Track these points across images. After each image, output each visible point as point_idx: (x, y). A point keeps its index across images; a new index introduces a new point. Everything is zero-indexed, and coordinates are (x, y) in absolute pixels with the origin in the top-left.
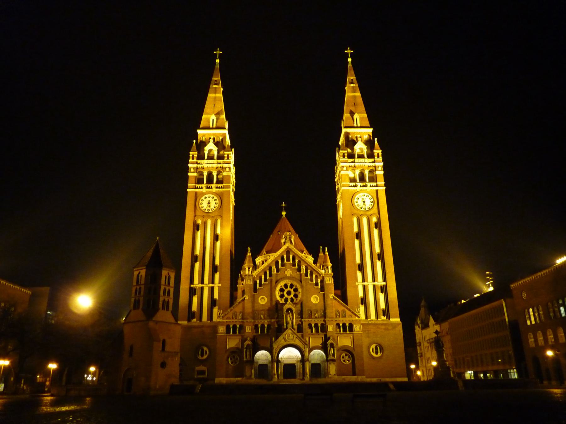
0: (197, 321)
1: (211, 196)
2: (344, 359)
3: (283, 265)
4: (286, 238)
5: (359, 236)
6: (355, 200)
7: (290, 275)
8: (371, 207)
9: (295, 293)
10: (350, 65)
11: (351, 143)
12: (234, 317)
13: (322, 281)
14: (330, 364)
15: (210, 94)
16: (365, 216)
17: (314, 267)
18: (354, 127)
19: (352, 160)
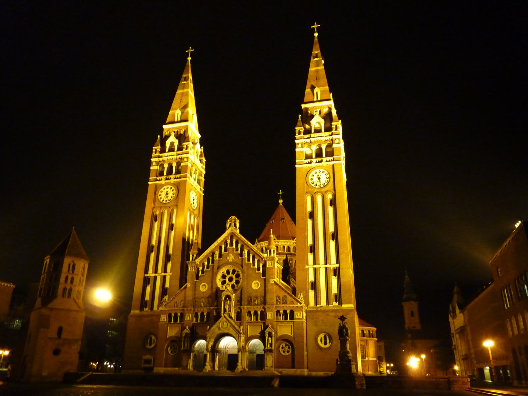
0: (148, 309)
1: (170, 186)
2: (283, 350)
3: (226, 250)
4: (231, 222)
5: (312, 215)
6: (310, 177)
7: (232, 260)
8: (326, 184)
9: (236, 279)
10: (316, 40)
11: (308, 117)
12: (176, 306)
13: (264, 266)
14: (267, 355)
15: (179, 90)
16: (320, 193)
17: (256, 251)
18: (313, 102)
19: (308, 136)
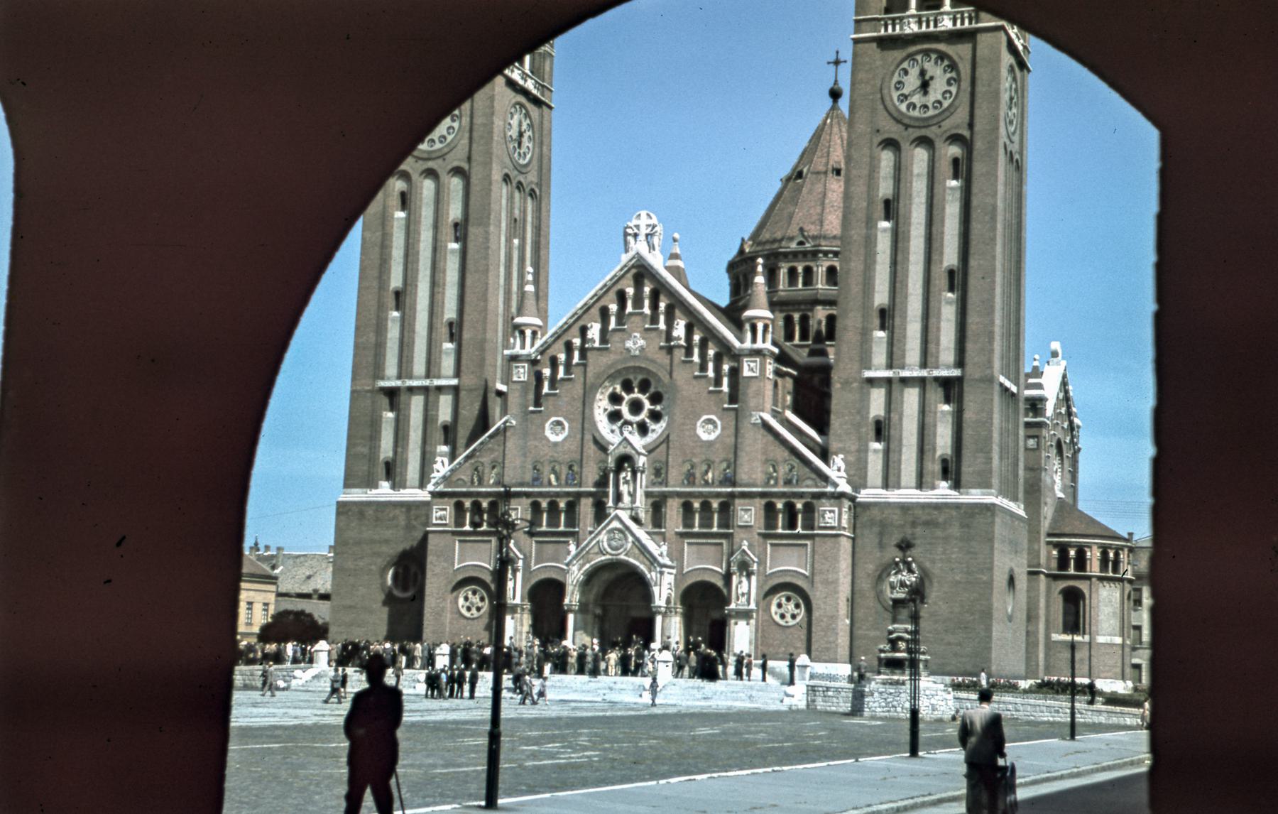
2: (782, 611)
13: (735, 373)
